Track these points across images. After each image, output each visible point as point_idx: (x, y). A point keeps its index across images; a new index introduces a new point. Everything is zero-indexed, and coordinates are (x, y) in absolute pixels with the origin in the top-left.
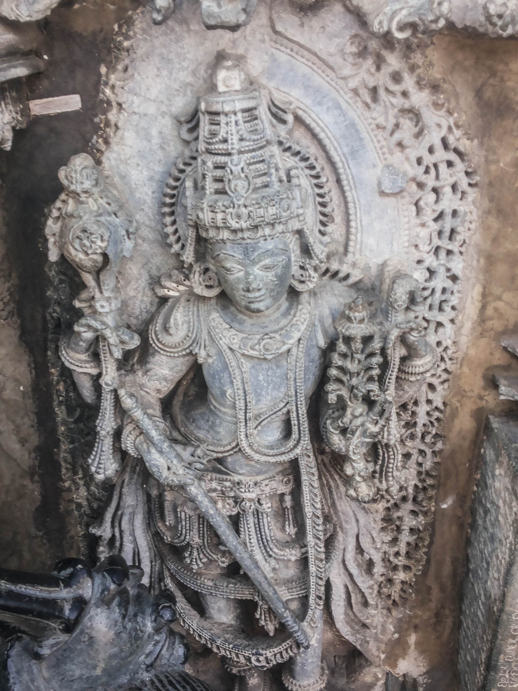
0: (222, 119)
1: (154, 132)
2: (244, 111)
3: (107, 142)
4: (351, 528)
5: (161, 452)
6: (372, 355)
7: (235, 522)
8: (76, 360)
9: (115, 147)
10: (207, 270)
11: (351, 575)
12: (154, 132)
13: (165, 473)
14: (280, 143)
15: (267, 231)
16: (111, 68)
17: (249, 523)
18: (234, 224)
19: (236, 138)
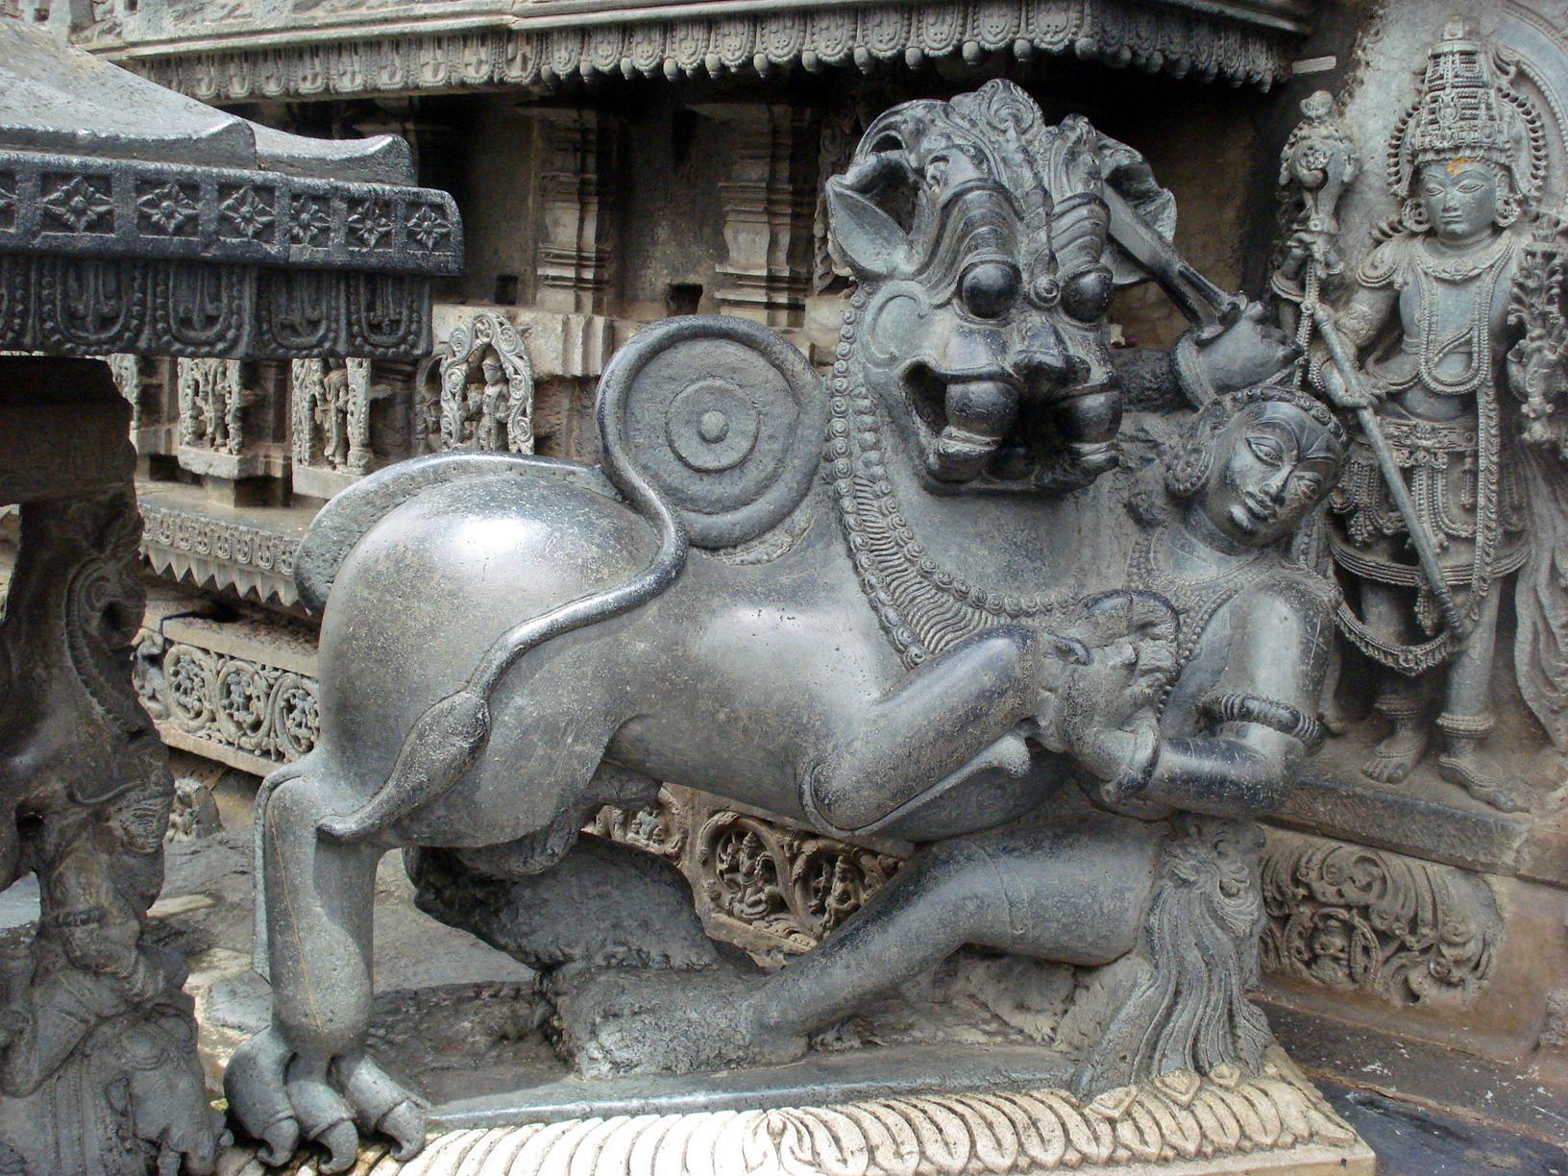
0: (1442, 60)
1: (1394, 86)
2: (1462, 53)
3: (1351, 95)
4: (1546, 537)
5: (1341, 371)
6: (1553, 273)
7: (1408, 474)
8: (1280, 285)
9: (1358, 100)
10: (1419, 206)
11: (1541, 607)
12: (1394, 86)
13: (1341, 393)
14: (1500, 90)
15: (1468, 153)
16: (1365, 32)
17: (1421, 480)
18: (1438, 144)
19: (1450, 74)
